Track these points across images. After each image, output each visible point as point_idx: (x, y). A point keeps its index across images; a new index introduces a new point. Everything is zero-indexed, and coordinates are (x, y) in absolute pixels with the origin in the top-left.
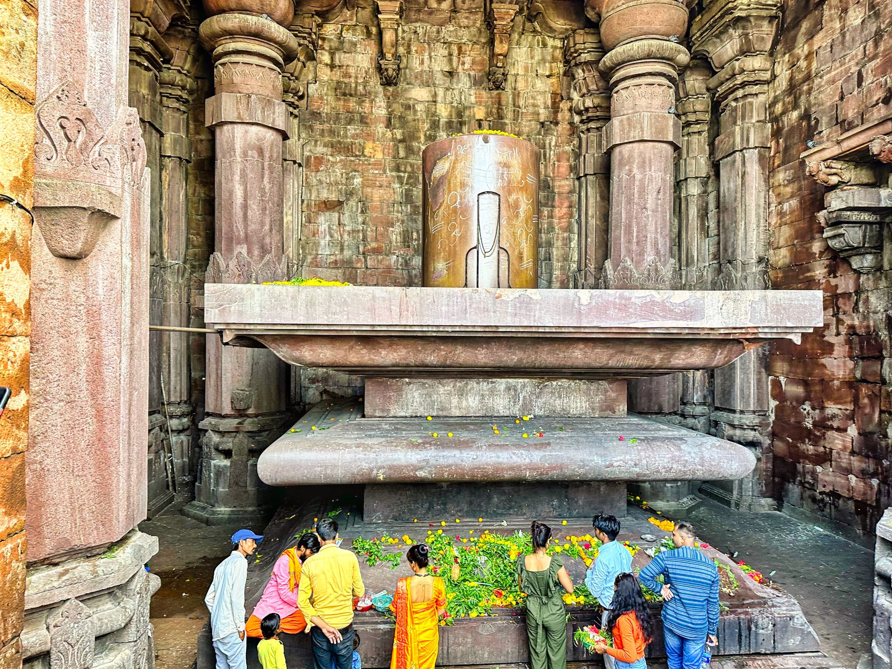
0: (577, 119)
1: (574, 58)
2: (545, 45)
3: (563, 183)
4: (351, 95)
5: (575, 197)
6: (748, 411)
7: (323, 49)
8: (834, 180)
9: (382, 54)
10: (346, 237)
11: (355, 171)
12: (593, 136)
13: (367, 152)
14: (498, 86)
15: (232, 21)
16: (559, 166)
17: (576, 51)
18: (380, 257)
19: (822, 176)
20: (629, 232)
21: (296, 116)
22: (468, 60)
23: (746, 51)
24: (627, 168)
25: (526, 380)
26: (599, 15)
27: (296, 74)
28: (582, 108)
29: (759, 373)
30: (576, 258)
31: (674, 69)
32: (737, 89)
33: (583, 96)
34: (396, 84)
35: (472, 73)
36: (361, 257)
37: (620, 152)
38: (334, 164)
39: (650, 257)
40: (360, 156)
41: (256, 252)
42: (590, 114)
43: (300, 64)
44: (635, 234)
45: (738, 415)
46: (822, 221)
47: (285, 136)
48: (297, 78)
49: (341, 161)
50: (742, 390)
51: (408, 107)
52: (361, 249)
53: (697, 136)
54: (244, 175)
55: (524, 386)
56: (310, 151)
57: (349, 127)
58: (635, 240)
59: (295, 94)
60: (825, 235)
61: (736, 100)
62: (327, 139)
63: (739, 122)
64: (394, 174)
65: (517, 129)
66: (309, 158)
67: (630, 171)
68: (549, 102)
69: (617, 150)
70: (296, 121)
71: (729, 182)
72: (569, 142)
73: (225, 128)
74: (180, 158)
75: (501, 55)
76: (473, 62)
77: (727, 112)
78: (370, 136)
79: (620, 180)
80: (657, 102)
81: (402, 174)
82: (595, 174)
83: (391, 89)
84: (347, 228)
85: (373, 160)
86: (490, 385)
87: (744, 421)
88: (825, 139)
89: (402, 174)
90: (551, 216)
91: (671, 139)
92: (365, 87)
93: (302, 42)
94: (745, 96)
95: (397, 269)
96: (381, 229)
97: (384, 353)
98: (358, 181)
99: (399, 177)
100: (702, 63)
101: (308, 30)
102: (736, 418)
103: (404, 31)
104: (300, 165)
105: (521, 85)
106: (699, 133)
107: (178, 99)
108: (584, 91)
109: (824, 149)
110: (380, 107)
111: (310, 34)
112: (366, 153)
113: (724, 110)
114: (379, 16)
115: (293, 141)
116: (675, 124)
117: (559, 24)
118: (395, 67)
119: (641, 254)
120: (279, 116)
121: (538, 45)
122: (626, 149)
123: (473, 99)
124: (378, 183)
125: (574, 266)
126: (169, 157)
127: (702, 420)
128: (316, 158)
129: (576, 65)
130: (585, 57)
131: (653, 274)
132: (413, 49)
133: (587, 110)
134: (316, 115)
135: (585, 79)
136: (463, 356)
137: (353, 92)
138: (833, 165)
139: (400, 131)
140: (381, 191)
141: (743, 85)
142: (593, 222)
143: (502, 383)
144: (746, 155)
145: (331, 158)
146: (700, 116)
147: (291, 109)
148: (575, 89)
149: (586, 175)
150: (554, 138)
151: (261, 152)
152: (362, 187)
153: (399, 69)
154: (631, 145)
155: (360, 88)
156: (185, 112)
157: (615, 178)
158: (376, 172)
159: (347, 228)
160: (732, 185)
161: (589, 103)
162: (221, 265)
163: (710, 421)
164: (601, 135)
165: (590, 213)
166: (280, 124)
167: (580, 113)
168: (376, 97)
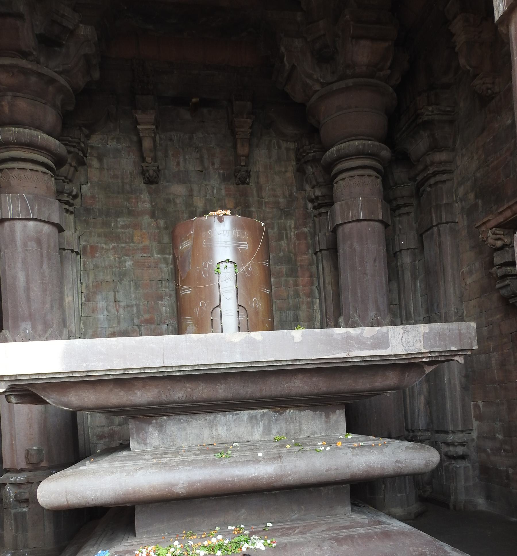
0: (310, 205)
2: (279, 147)
3: (305, 257)
4: (118, 193)
5: (314, 269)
7: (92, 155)
12: (322, 218)
13: (136, 239)
14: (243, 181)
16: (299, 244)
27: (70, 177)
28: (313, 197)
32: (430, 178)
33: (313, 187)
34: (157, 183)
35: (221, 171)
38: (107, 250)
42: (320, 202)
43: (72, 169)
48: (71, 181)
51: (168, 201)
57: (119, 219)
59: (69, 194)
62: (100, 230)
64: (159, 256)
68: (287, 193)
69: (340, 229)
78: (136, 226)
81: (167, 256)
82: (327, 249)
83: (153, 186)
85: (141, 245)
90: (296, 285)
92: (131, 185)
93: (72, 149)
99: (165, 259)
105: (262, 180)
108: (314, 183)
112: (135, 240)
114: (139, 127)
115: (68, 233)
121: (274, 147)
123: (223, 192)
129: (306, 162)
133: (317, 198)
134: (88, 211)
135: (313, 173)
139: (163, 221)
140: (150, 271)
142: (330, 288)
144: (441, 229)
147: (67, 207)
148: (307, 182)
149: (321, 251)
150: (293, 222)
155: (127, 187)
161: (318, 193)
165: (327, 281)
167: (312, 201)
168: (141, 193)
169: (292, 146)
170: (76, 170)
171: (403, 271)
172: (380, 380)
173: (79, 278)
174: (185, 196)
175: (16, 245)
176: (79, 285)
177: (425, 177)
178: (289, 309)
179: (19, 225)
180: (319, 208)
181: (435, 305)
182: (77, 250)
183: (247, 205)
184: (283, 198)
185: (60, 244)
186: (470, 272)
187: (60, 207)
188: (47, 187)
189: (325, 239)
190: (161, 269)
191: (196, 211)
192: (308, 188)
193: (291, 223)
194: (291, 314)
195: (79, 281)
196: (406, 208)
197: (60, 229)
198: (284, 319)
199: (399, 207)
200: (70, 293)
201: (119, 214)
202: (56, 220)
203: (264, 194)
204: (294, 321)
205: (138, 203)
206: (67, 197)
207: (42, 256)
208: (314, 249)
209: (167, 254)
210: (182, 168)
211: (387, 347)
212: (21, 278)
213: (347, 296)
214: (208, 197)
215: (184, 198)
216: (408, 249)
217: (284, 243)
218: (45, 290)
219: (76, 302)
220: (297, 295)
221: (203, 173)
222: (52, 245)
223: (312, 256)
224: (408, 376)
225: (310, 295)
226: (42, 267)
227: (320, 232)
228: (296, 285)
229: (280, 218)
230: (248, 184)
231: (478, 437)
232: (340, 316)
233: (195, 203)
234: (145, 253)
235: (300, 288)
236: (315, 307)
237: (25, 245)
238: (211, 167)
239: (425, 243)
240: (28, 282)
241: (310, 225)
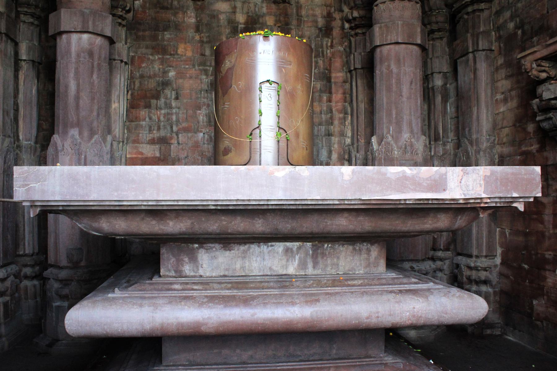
0: (347, 25)
5: (347, 86)
6: (482, 256)
8: (544, 75)
11: (170, 67)
13: (180, 51)
18: (190, 135)
19: (534, 72)
20: (389, 114)
21: (124, 26)
24: (386, 64)
28: (351, 18)
29: (490, 226)
30: (349, 134)
36: (174, 135)
37: (381, 51)
38: (153, 61)
39: (406, 136)
40: (174, 55)
41: (86, 134)
42: (357, 23)
44: (394, 116)
45: (474, 259)
46: (535, 107)
49: (159, 58)
50: (477, 240)
52: (175, 129)
53: (439, 41)
54: (77, 73)
56: (134, 52)
57: (166, 33)
58: (394, 121)
59: (124, 9)
60: (538, 118)
61: (468, 14)
63: (470, 31)
65: (300, 33)
67: (389, 66)
68: (325, 13)
69: (378, 50)
71: (464, 76)
74: (33, 61)
77: (461, 23)
79: (382, 73)
80: (407, 14)
81: (208, 68)
82: (362, 68)
87: (478, 264)
88: (535, 43)
89: (208, 68)
90: (330, 100)
91: (419, 42)
95: (204, 144)
96: (190, 112)
98: (172, 74)
104: (126, 63)
107: (33, 15)
108: (352, 4)
109: (535, 52)
110: (191, 17)
113: (459, 21)
116: (422, 31)
122: (385, 49)
123: (265, 10)
124: (188, 75)
125: (348, 141)
126: (25, 60)
127: (447, 262)
128: (139, 57)
131: (408, 148)
133: (354, 19)
137: (169, 6)
138: (543, 64)
140: (191, 82)
142: (362, 106)
147: (120, 21)
148: (345, 4)
149: (355, 69)
150: (330, 40)
152: (176, 79)
154: (388, 47)
156: (37, 26)
157: (377, 72)
158: (187, 67)
160: (466, 78)
161: (356, 14)
162: (58, 145)
163: (453, 263)
164: (365, 39)
167: (349, 21)
171: (434, 95)
172: (430, 222)
173: (126, 86)
174: (229, 12)
175: (71, 55)
176: (126, 92)
177: (463, 5)
178: (320, 124)
179: (74, 37)
180: (356, 29)
181: (467, 129)
182: (126, 60)
183: (287, 24)
184: (322, 17)
185: (111, 54)
186: (505, 100)
187: (113, 21)
188: (103, 3)
189: (360, 58)
190: (201, 80)
191: (237, 27)
192: (346, 9)
194: (323, 128)
195: (126, 89)
196: (440, 33)
197: (111, 41)
199: (432, 32)
200: (116, 101)
202: (108, 33)
204: (325, 135)
205: (184, 18)
207: (93, 67)
208: (349, 67)
209: (207, 66)
213: (382, 116)
215: (228, 14)
216: (440, 73)
218: (93, 99)
219: (122, 109)
222: (103, 56)
223: (346, 74)
224: (461, 219)
226: (92, 76)
227: (356, 51)
231: (501, 264)
232: (372, 135)
233: (237, 19)
234: (187, 65)
235: (333, 104)
236: (346, 122)
237: (78, 56)
239: (460, 69)
241: (346, 44)
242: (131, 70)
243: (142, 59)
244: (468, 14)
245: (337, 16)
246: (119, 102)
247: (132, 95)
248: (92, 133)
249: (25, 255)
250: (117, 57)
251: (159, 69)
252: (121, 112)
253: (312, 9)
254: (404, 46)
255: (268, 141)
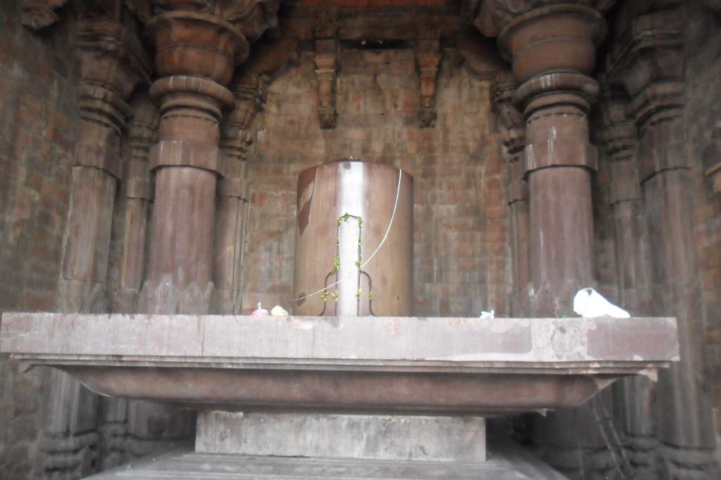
0: (505, 149)
1: (498, 95)
2: (472, 86)
3: (497, 208)
9: (320, 104)
10: (284, 264)
15: (171, 82)
17: (498, 89)
21: (244, 159)
22: (400, 103)
23: (657, 78)
25: (371, 417)
26: (511, 56)
27: (246, 122)
30: (510, 280)
31: (584, 97)
33: (509, 128)
43: (249, 115)
47: (219, 177)
49: (283, 195)
51: (344, 146)
55: (368, 424)
61: (653, 124)
66: (254, 196)
68: (478, 136)
69: (532, 176)
70: (243, 164)
72: (498, 171)
73: (164, 171)
75: (427, 97)
76: (406, 105)
83: (329, 131)
84: (286, 255)
86: (331, 422)
91: (583, 162)
94: (660, 120)
97: (190, 385)
100: (621, 93)
101: (254, 87)
102: (681, 456)
103: (342, 82)
104: (245, 201)
105: (450, 122)
106: (628, 157)
108: (510, 124)
111: (256, 89)
116: (588, 151)
117: (483, 67)
118: (332, 112)
119: (561, 275)
120: (212, 158)
122: (540, 174)
123: (405, 136)
125: (509, 289)
126: (133, 198)
129: (501, 101)
130: (506, 94)
132: (351, 96)
133: (513, 140)
134: (261, 157)
136: (273, 390)
141: (659, 109)
143: (344, 419)
145: (273, 193)
146: (626, 142)
147: (238, 153)
151: (192, 189)
153: (336, 115)
154: (544, 171)
157: (532, 204)
159: (286, 255)
161: (513, 134)
166: (213, 166)
167: (507, 144)
169: (486, 84)
170: (253, 116)
183: (431, 150)
193: (481, 169)
194: (476, 274)
198: (468, 280)
201: (292, 160)
203: (451, 137)
206: (241, 143)
210: (362, 111)
211: (529, 349)
212: (169, 227)
214: (388, 141)
217: (472, 193)
220: (484, 251)
221: (384, 115)
225: (501, 251)
228: (484, 240)
229: (468, 164)
230: (434, 126)
238: (393, 109)
240: (175, 232)
241: (505, 171)
242: (251, 209)
243: (263, 196)
244: (653, 124)
245: (492, 138)
246: (235, 245)
247: (251, 235)
248: (189, 278)
249: (116, 422)
250: (233, 195)
251: (283, 207)
252: (237, 256)
253: (462, 132)
254: (562, 170)
255: (349, 288)
